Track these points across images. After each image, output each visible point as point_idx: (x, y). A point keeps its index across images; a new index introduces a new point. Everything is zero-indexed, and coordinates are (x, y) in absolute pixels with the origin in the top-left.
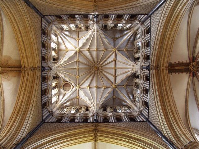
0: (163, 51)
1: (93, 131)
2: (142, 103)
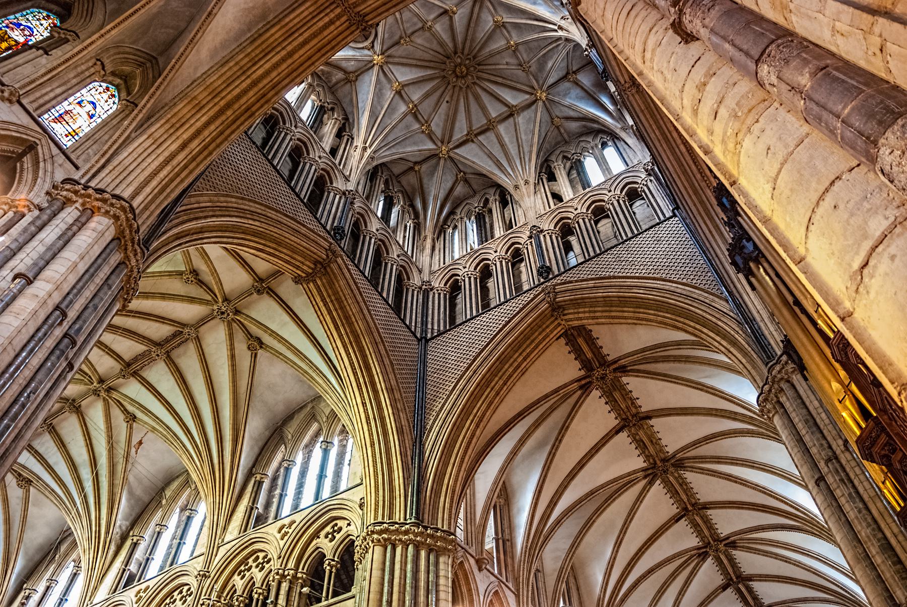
1: (316, 263)
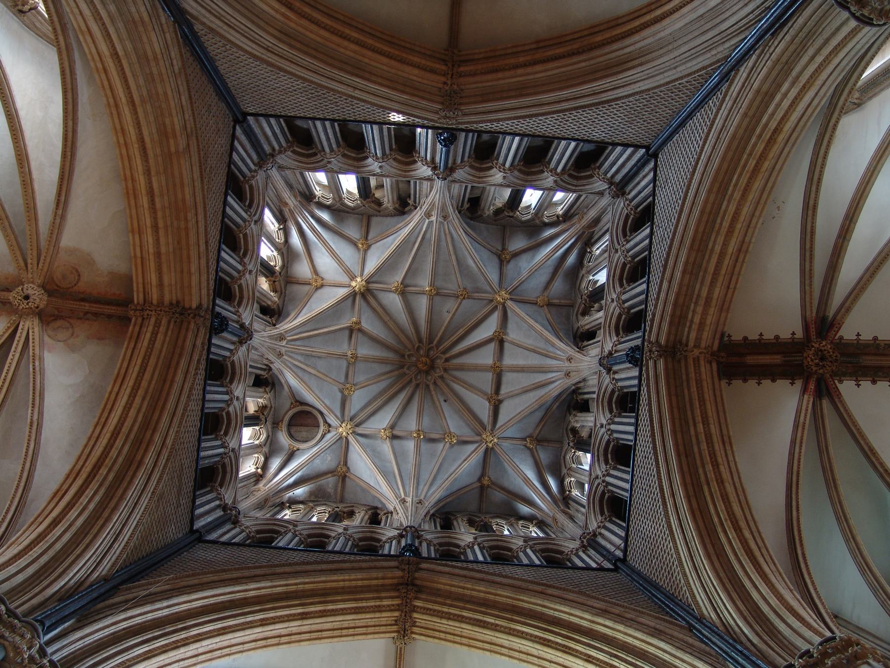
0: (702, 283)
1: (395, 587)
2: (597, 502)
